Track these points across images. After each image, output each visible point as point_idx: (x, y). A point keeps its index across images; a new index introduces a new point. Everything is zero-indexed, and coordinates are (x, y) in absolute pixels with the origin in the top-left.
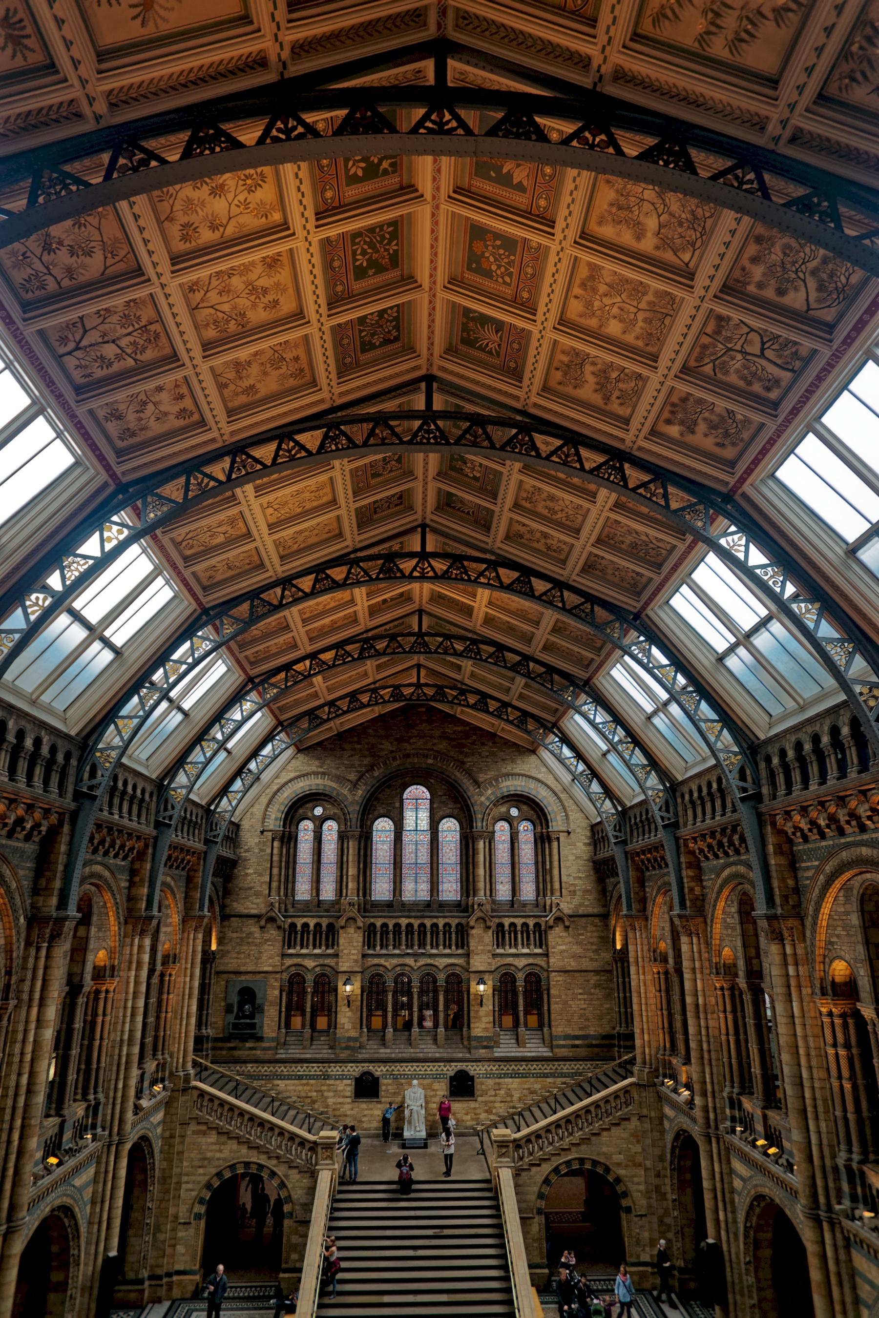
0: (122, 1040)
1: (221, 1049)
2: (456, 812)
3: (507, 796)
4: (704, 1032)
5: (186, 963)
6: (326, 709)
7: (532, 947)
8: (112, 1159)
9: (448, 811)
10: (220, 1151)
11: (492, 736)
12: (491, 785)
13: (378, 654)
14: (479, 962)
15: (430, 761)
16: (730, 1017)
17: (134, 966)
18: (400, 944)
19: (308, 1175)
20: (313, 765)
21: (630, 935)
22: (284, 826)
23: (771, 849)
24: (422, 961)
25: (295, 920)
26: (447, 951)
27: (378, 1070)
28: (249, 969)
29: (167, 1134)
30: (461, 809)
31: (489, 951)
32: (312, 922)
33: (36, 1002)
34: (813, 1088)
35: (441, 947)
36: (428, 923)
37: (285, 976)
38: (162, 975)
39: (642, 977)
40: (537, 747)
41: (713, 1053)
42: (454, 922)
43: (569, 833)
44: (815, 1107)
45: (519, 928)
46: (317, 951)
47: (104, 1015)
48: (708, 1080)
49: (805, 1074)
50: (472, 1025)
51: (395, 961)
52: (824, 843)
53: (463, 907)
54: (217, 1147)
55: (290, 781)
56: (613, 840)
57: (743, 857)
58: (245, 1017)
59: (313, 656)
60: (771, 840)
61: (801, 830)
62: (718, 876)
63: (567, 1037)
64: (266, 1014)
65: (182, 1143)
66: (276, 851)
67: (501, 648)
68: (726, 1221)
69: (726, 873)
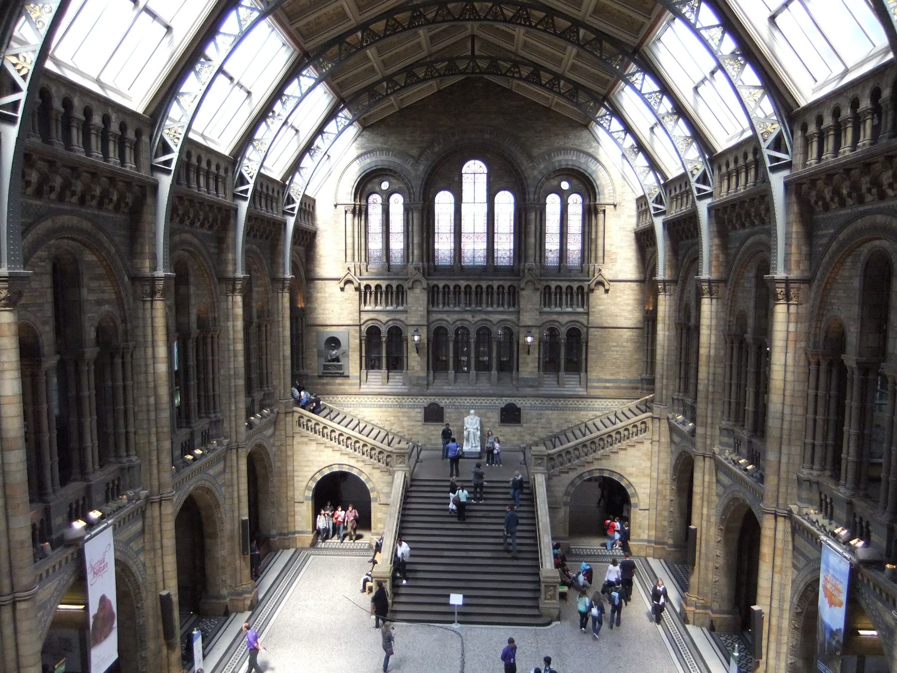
1: (317, 384)
3: (559, 170)
5: (278, 317)
7: (575, 306)
8: (234, 457)
10: (320, 456)
11: (547, 112)
14: (529, 318)
18: (459, 303)
19: (388, 473)
22: (355, 201)
24: (479, 317)
26: (501, 309)
27: (443, 402)
31: (537, 310)
33: (150, 344)
35: (495, 306)
36: (484, 285)
38: (259, 326)
40: (590, 122)
42: (507, 284)
43: (615, 206)
45: (564, 290)
46: (389, 308)
47: (213, 356)
50: (520, 369)
51: (456, 317)
52: (842, 212)
53: (514, 271)
54: (317, 453)
56: (653, 212)
57: (766, 227)
58: (333, 360)
61: (824, 199)
62: (742, 244)
64: (350, 358)
69: (749, 241)
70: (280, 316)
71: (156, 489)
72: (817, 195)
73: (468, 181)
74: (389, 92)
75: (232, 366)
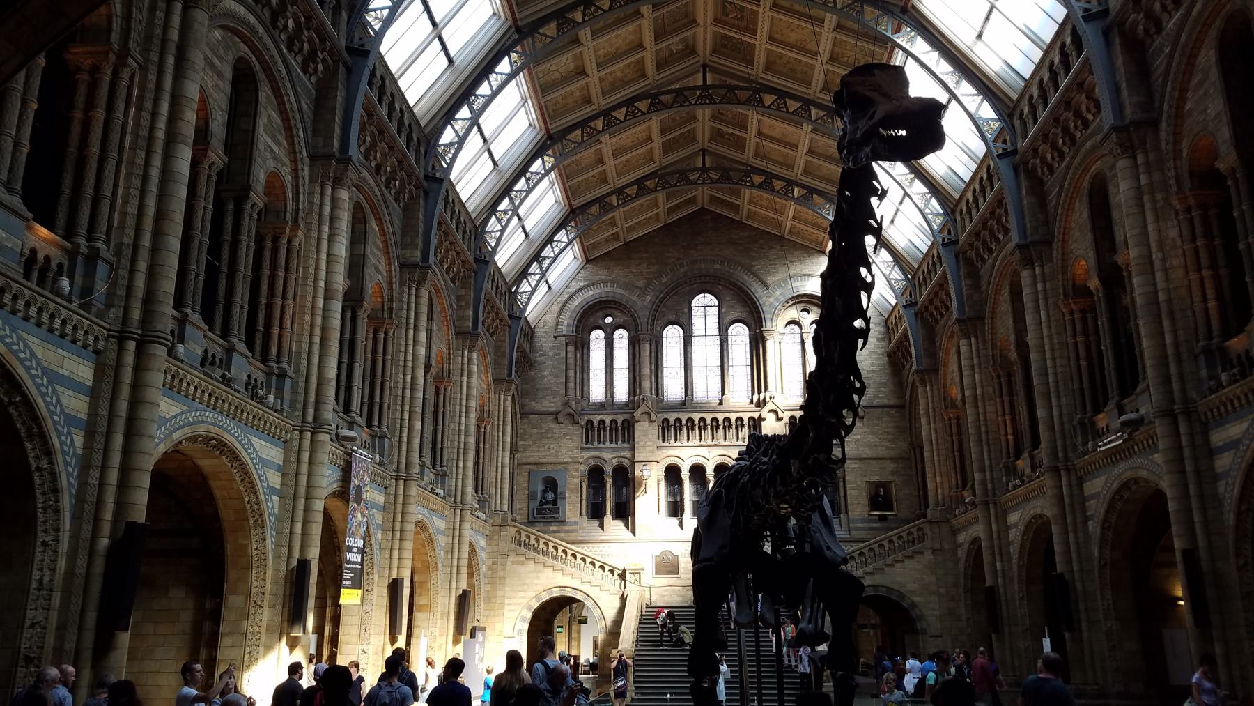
0: (459, 430)
2: (744, 315)
4: (981, 417)
5: (498, 420)
6: (614, 199)
8: (458, 519)
9: (736, 315)
10: (538, 578)
12: (779, 286)
13: (665, 107)
15: (718, 266)
16: (1006, 399)
17: (466, 373)
20: (603, 275)
21: (920, 390)
23: (1024, 192)
25: (591, 417)
28: (550, 461)
29: (490, 562)
30: (751, 312)
32: (608, 419)
34: (1056, 374)
36: (721, 417)
37: (582, 467)
39: (933, 426)
41: (990, 434)
42: (746, 416)
44: (1057, 387)
46: (613, 445)
48: (986, 457)
49: (1049, 364)
54: (535, 575)
55: (580, 290)
58: (547, 503)
59: (606, 113)
60: (1024, 184)
63: (863, 521)
65: (504, 570)
66: (570, 355)
67: (782, 95)
68: (1003, 570)
70: (501, 419)
71: (403, 466)
72: (1041, 162)
73: (698, 313)
74: (620, 202)
75: (463, 419)
